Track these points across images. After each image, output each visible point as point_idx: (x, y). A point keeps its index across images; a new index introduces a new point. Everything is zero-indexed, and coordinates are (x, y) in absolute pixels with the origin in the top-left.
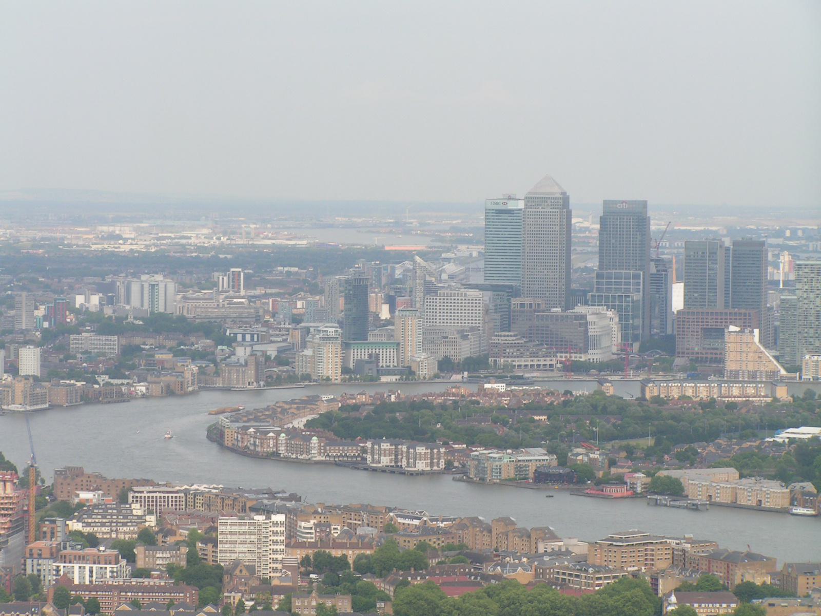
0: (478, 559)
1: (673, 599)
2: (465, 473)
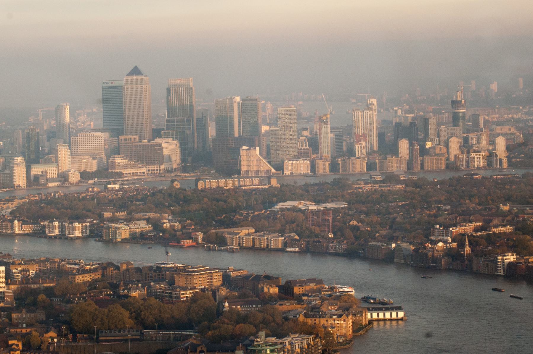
0: (114, 287)
1: (227, 304)
2: (101, 236)
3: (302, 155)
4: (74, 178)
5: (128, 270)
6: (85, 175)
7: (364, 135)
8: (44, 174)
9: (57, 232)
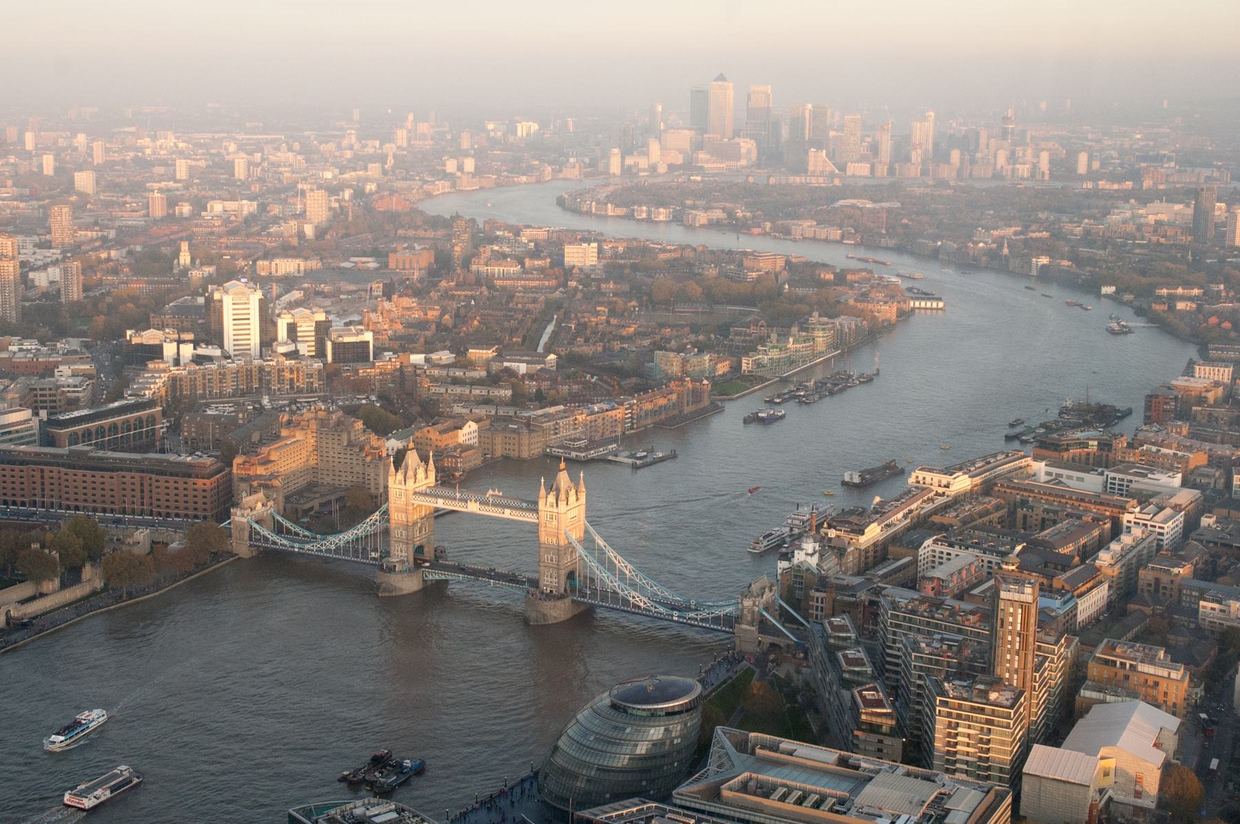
0: (690, 265)
3: (863, 159)
4: (662, 169)
5: (703, 252)
6: (671, 167)
7: (920, 144)
8: (636, 164)
9: (644, 215)
